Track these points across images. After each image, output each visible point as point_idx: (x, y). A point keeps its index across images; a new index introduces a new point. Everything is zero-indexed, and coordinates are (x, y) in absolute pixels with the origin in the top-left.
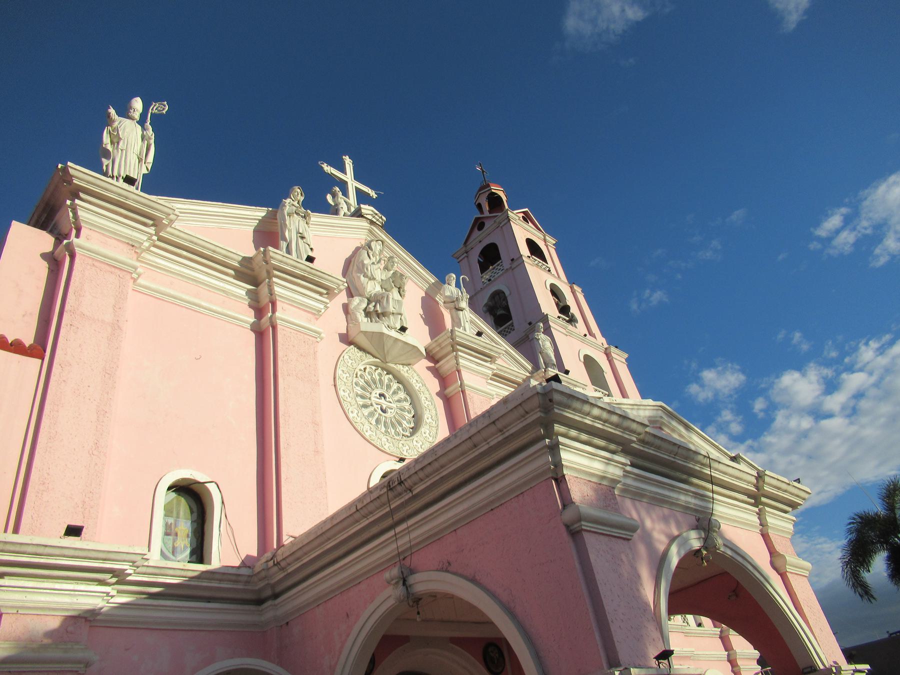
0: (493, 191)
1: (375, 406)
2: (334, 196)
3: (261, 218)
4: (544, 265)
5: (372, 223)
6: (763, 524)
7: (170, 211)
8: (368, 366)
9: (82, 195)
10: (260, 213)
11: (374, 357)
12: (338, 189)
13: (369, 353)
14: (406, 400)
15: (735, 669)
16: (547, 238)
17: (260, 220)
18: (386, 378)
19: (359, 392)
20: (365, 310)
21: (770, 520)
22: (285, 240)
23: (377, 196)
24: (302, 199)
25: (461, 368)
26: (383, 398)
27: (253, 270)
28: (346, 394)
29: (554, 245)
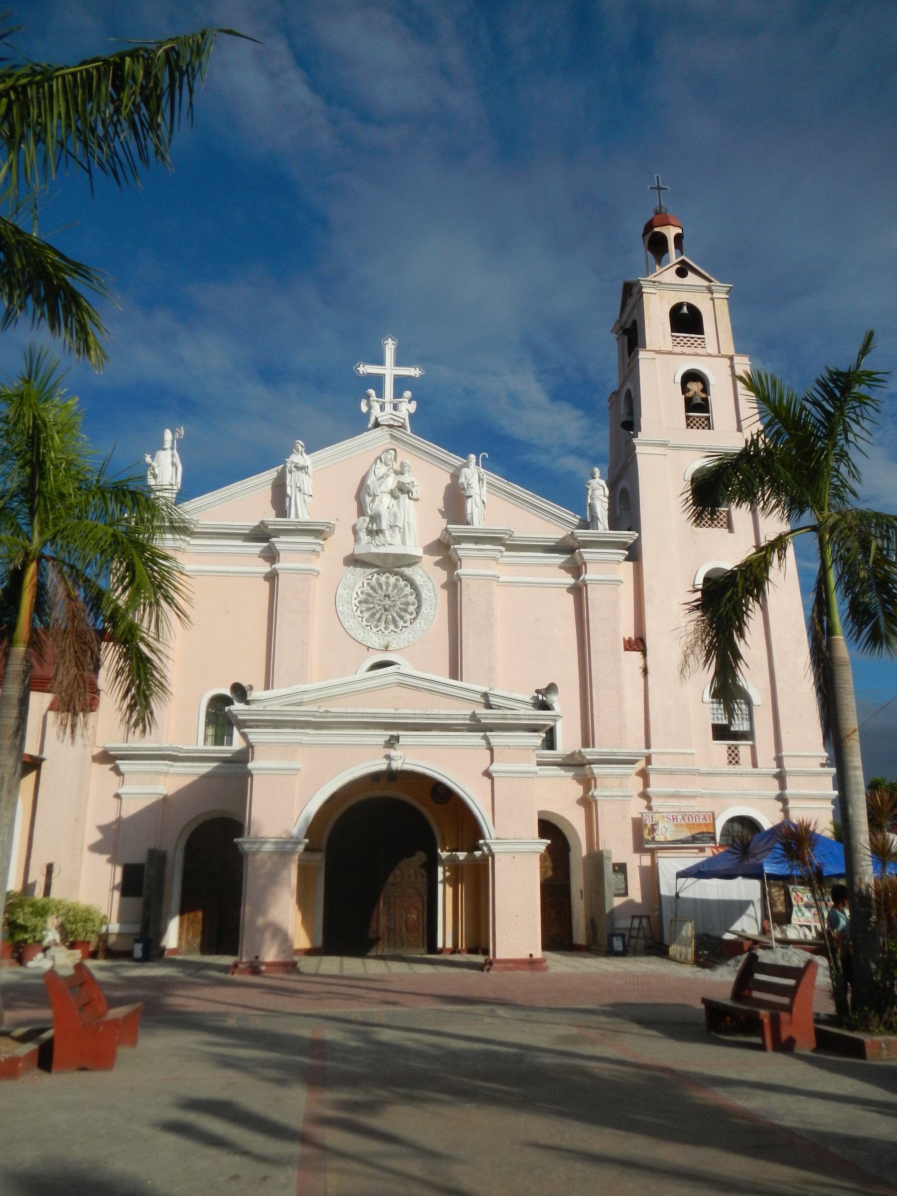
0: (656, 230)
1: (378, 607)
2: (368, 397)
3: (275, 476)
5: (391, 426)
6: (489, 743)
10: (271, 475)
11: (377, 566)
12: (372, 392)
14: (412, 594)
16: (713, 288)
17: (275, 478)
18: (392, 580)
20: (367, 528)
21: (493, 741)
22: (288, 496)
24: (304, 449)
25: (461, 558)
26: (387, 598)
27: (263, 531)
28: (345, 608)
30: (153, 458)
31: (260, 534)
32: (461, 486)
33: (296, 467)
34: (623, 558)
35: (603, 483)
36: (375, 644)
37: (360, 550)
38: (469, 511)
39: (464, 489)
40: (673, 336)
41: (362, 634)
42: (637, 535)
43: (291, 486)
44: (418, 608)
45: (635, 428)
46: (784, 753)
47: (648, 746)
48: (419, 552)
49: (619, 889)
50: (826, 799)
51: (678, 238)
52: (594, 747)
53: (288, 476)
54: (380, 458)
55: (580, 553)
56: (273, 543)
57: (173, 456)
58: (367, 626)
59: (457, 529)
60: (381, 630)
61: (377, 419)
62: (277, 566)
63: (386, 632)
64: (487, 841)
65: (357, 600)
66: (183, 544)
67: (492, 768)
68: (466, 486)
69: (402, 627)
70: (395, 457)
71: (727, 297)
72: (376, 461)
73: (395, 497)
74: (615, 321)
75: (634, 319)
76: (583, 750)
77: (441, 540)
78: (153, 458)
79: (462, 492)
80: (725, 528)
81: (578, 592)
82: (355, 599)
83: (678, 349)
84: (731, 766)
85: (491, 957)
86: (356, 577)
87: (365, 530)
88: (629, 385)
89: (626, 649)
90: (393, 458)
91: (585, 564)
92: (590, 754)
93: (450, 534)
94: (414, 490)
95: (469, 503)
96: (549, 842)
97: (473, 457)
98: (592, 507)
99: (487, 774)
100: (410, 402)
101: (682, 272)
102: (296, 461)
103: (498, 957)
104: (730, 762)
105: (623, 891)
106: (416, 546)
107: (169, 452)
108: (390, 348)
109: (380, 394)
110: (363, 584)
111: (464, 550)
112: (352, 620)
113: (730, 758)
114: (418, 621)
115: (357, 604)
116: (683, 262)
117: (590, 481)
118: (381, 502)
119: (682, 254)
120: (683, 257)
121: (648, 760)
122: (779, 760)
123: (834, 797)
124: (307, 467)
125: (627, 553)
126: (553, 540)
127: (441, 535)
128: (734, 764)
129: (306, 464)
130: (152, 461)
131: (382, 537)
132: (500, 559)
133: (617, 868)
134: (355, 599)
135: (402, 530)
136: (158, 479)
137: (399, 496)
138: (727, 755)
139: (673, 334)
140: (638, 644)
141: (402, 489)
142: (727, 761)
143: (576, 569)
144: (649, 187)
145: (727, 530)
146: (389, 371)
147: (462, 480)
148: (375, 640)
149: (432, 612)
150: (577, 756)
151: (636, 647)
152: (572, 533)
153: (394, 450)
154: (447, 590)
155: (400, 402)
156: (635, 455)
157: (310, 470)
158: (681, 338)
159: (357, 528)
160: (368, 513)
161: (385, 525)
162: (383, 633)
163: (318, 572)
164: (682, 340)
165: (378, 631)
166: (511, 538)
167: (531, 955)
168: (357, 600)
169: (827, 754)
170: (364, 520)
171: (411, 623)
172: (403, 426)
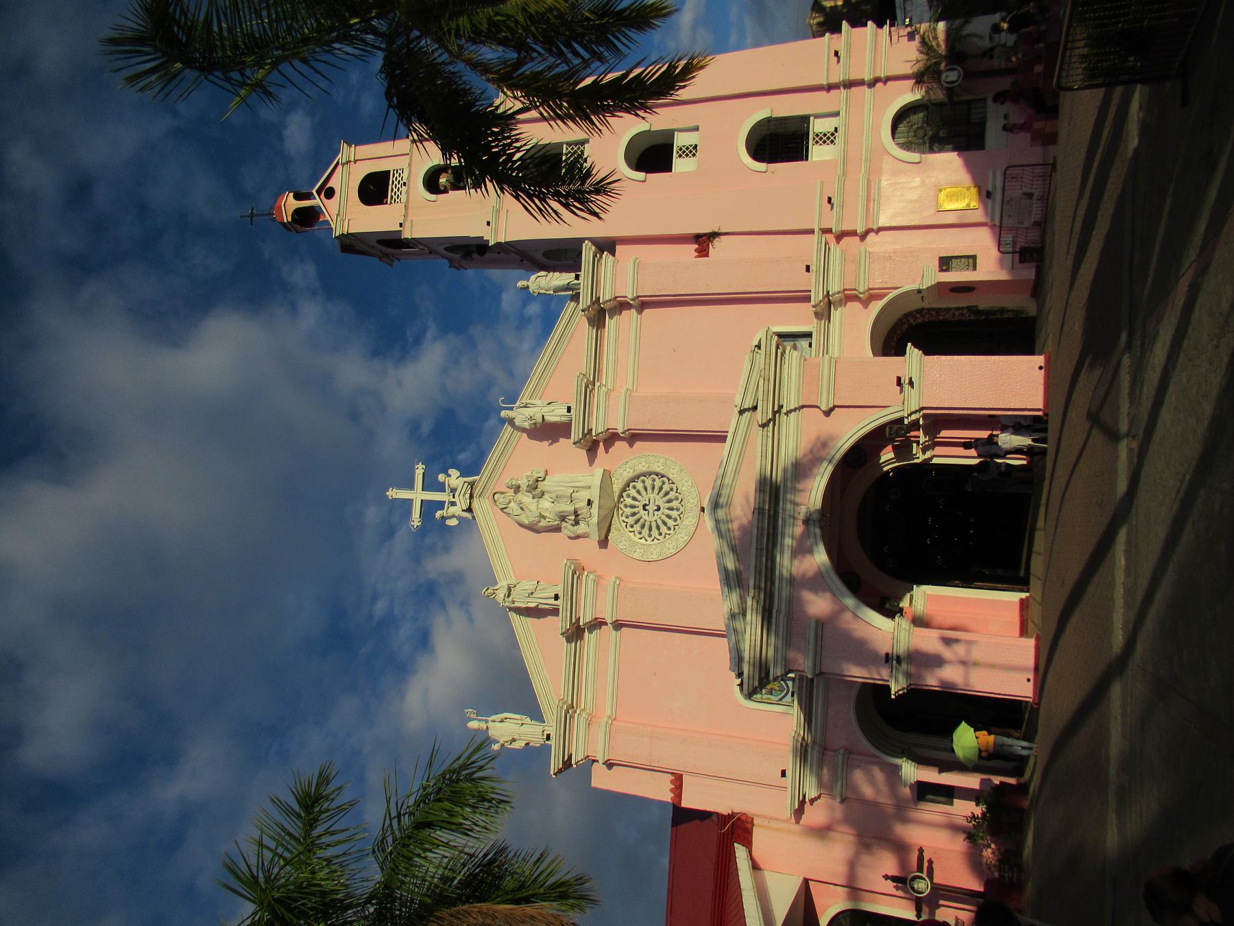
0: (290, 219)
2: (444, 518)
4: (393, 182)
5: (471, 497)
6: (795, 410)
7: (559, 708)
8: (621, 518)
9: (566, 759)
12: (438, 514)
13: (611, 522)
15: (884, 80)
19: (648, 532)
23: (420, 463)
24: (491, 588)
26: (646, 507)
28: (655, 552)
29: (349, 145)
30: (497, 742)
31: (575, 633)
32: (533, 426)
33: (509, 596)
34: (611, 257)
35: (533, 278)
36: (693, 522)
37: (595, 537)
38: (557, 419)
39: (535, 424)
40: (391, 203)
41: (683, 535)
42: (586, 242)
43: (528, 602)
44: (657, 475)
45: (480, 243)
46: (825, 83)
47: (811, 232)
48: (598, 472)
50: (876, 35)
51: (298, 197)
52: (810, 291)
53: (516, 605)
54: (502, 509)
55: (604, 303)
56: (585, 624)
57: (494, 721)
58: (675, 529)
59: (576, 433)
60: (679, 515)
61: (463, 511)
62: (609, 621)
63: (682, 509)
64: (906, 415)
65: (648, 538)
66: (584, 715)
67: (824, 408)
68: (533, 422)
69: (677, 492)
70: (502, 493)
71: (353, 146)
72: (505, 513)
73: (543, 494)
74: (380, 262)
75: (375, 243)
76: (813, 303)
77: (587, 448)
78: (497, 742)
79: (538, 426)
80: (584, 148)
81: (643, 305)
82: (646, 540)
83: (403, 197)
84: (836, 141)
85: (1040, 413)
86: (623, 539)
87: (576, 527)
88: (441, 249)
89: (707, 255)
90: (503, 496)
91: (616, 297)
92: (817, 294)
93: (581, 439)
94: (536, 475)
95: (549, 418)
96: (909, 344)
97: (503, 414)
98: (557, 290)
99: (827, 413)
100: (449, 476)
101: (330, 193)
102: (502, 596)
103: (1041, 407)
104: (832, 142)
105: (971, 261)
106: (593, 476)
107: (490, 724)
108: (395, 493)
109: (440, 505)
110: (631, 532)
111: (598, 427)
112: (667, 545)
113: (828, 142)
114: (671, 476)
115: (653, 538)
116: (319, 192)
117: (531, 291)
118: (547, 509)
119: (313, 193)
120: (314, 192)
121: (827, 231)
122: (830, 88)
123: (875, 26)
124: (508, 585)
125: (605, 253)
126: (590, 331)
127: (582, 448)
128: (835, 138)
129: (506, 587)
130: (498, 742)
131: (583, 511)
132: (609, 388)
133: (944, 268)
134: (646, 540)
135: (576, 489)
136: (516, 737)
137: (542, 491)
138: (825, 146)
139: (389, 203)
140: (703, 242)
141: (534, 488)
142: (831, 146)
143: (621, 306)
144: (250, 226)
145: (586, 146)
146: (417, 495)
147: (526, 425)
148: (689, 521)
149: (662, 460)
150: (819, 309)
151: (705, 244)
152: (582, 311)
153: (494, 494)
154: (635, 443)
155: (449, 485)
156: (506, 242)
157: (513, 582)
158: (393, 194)
159: (573, 535)
160: (558, 524)
161: (571, 508)
162: (682, 513)
163: (617, 578)
164: (395, 193)
165: (680, 518)
166: (588, 376)
167: (1040, 368)
168: (648, 538)
169: (827, 34)
170: (566, 528)
171: (673, 483)
172: (472, 484)
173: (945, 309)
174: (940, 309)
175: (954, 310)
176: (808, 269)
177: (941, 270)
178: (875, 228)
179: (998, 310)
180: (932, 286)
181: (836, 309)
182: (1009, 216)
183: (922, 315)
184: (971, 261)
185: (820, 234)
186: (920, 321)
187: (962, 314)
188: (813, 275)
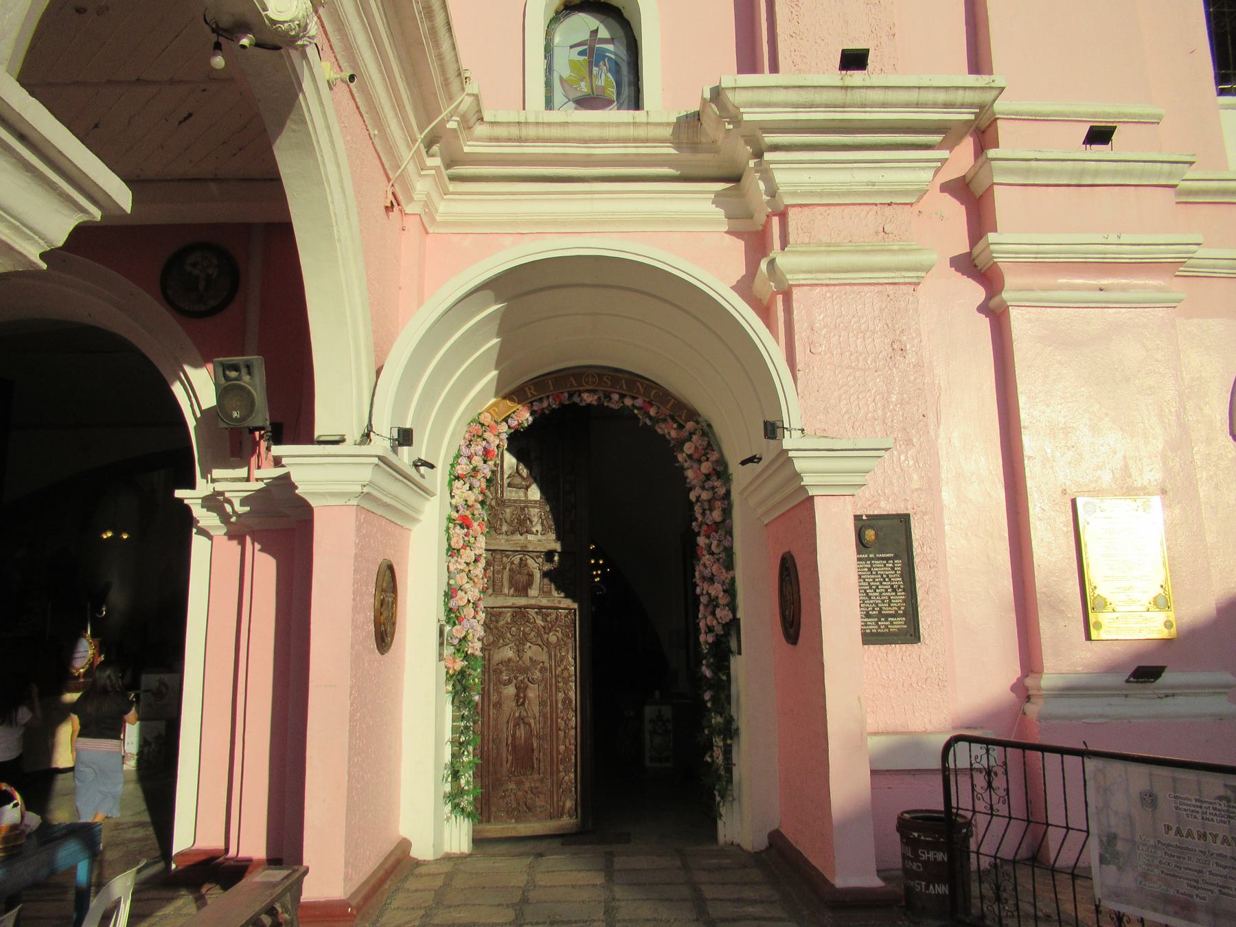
49: (881, 615)
105: (899, 623)
133: (870, 535)
173: (729, 551)
174: (729, 533)
175: (725, 576)
176: (854, 60)
177: (862, 524)
178: (1005, 295)
179: (729, 720)
180: (797, 476)
181: (719, 199)
182: (1149, 799)
183: (708, 477)
184: (899, 623)
185: (970, 97)
186: (690, 474)
187: (713, 603)
188: (835, 77)
